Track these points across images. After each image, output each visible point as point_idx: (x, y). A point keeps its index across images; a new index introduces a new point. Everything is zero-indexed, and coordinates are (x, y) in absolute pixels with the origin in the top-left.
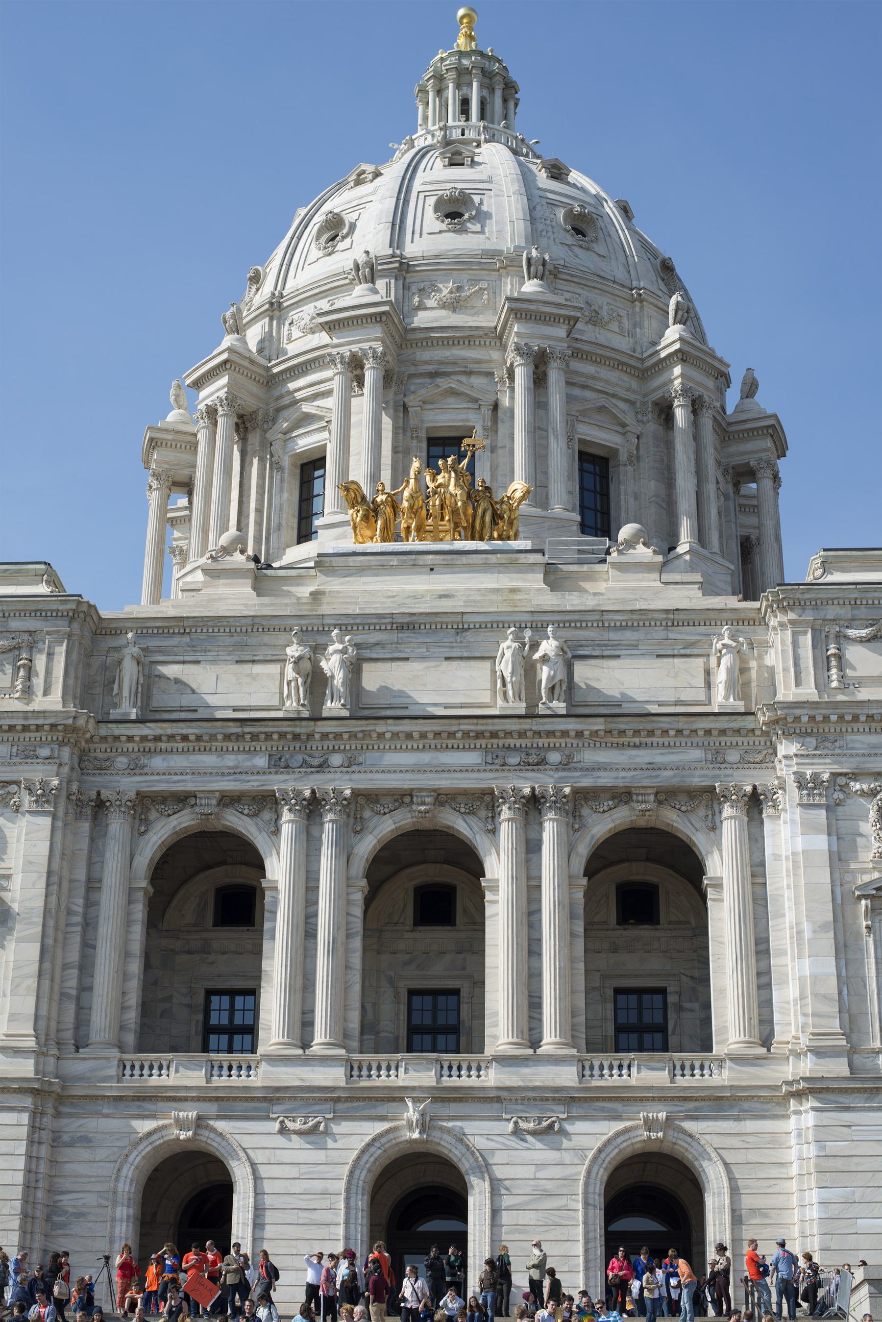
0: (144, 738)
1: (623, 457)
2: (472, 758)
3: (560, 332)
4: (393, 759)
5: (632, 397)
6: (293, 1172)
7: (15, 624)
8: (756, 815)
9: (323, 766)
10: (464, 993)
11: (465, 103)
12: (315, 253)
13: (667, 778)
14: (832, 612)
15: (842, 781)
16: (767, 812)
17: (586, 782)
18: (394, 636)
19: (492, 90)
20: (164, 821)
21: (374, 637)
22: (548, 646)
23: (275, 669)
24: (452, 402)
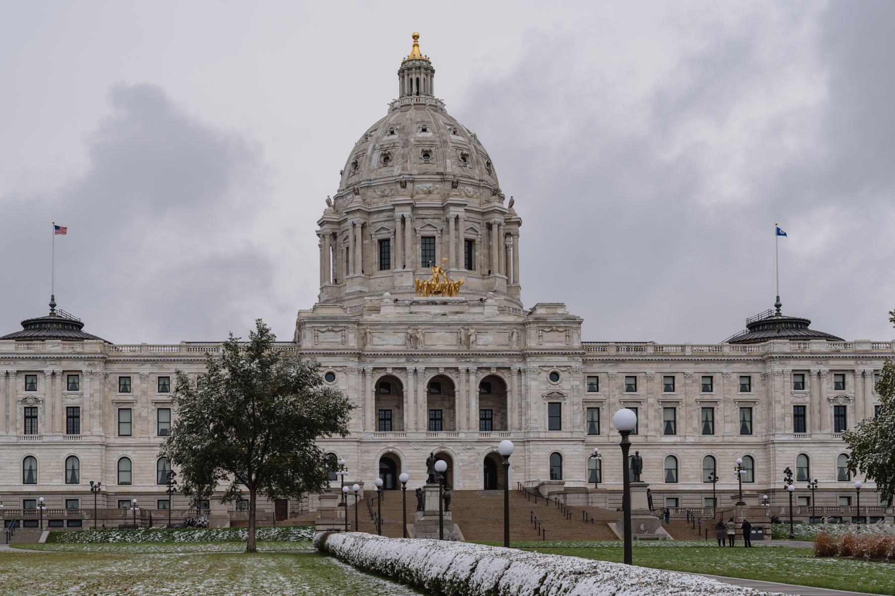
0: (374, 354)
1: (477, 242)
2: (453, 360)
3: (462, 209)
4: (434, 360)
5: (479, 221)
6: (415, 458)
7: (340, 325)
8: (519, 378)
9: (417, 362)
10: (443, 411)
11: (418, 80)
12: (382, 165)
13: (500, 365)
14: (541, 325)
15: (541, 368)
16: (522, 374)
17: (480, 366)
18: (433, 327)
19: (427, 75)
20: (378, 374)
21: (427, 327)
22: (472, 331)
23: (403, 335)
24: (428, 228)
